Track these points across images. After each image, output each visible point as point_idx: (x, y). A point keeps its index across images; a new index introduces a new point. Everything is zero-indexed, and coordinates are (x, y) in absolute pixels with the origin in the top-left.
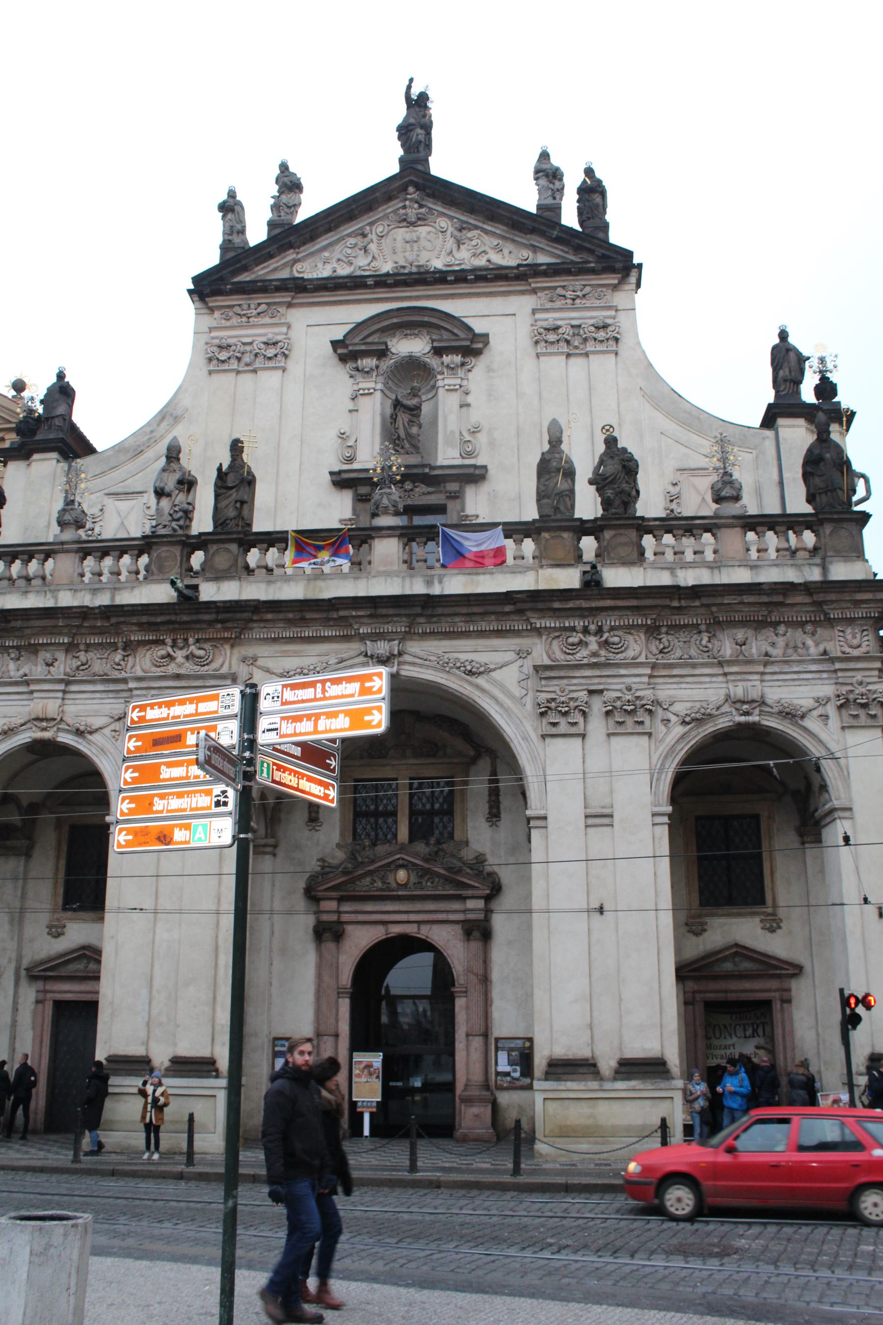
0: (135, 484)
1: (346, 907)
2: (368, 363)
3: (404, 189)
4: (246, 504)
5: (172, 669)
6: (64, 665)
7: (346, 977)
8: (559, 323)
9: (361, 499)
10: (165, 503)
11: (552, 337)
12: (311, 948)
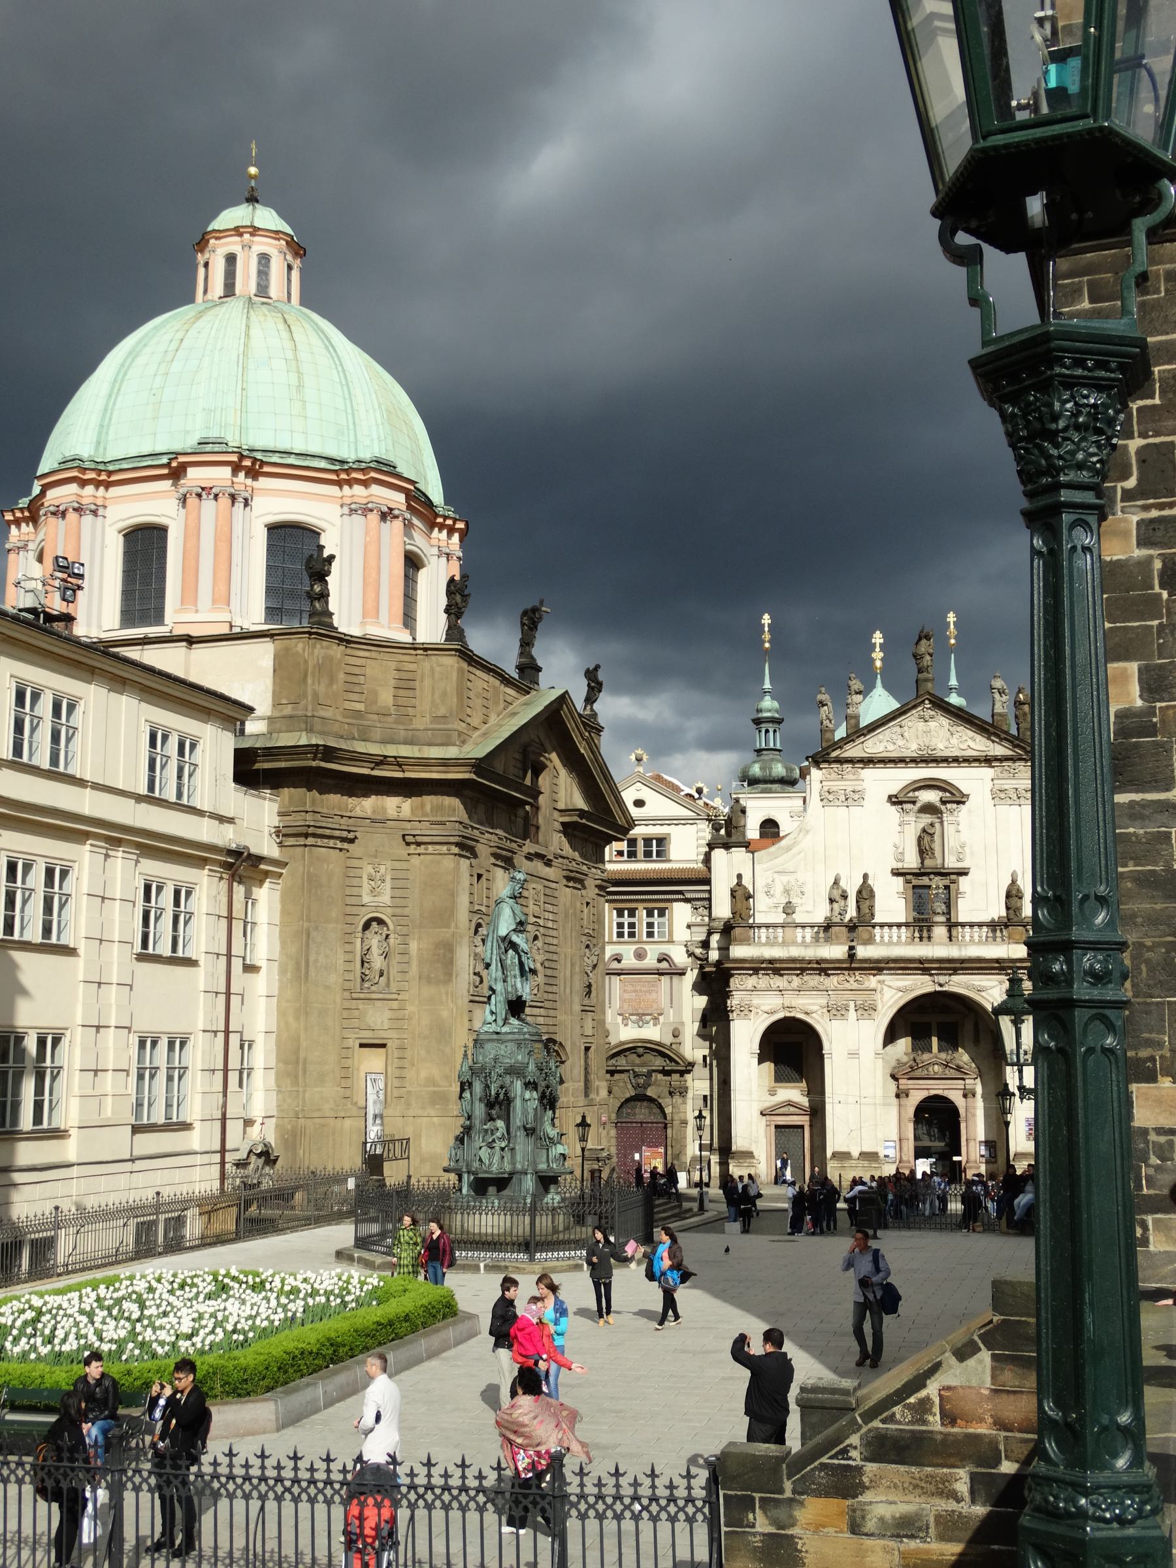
0: (790, 866)
1: (911, 1082)
2: (909, 806)
3: (923, 702)
4: (871, 907)
5: (848, 986)
6: (796, 981)
7: (911, 1112)
8: (1006, 787)
9: (908, 882)
10: (835, 905)
11: (1003, 795)
12: (895, 1101)
